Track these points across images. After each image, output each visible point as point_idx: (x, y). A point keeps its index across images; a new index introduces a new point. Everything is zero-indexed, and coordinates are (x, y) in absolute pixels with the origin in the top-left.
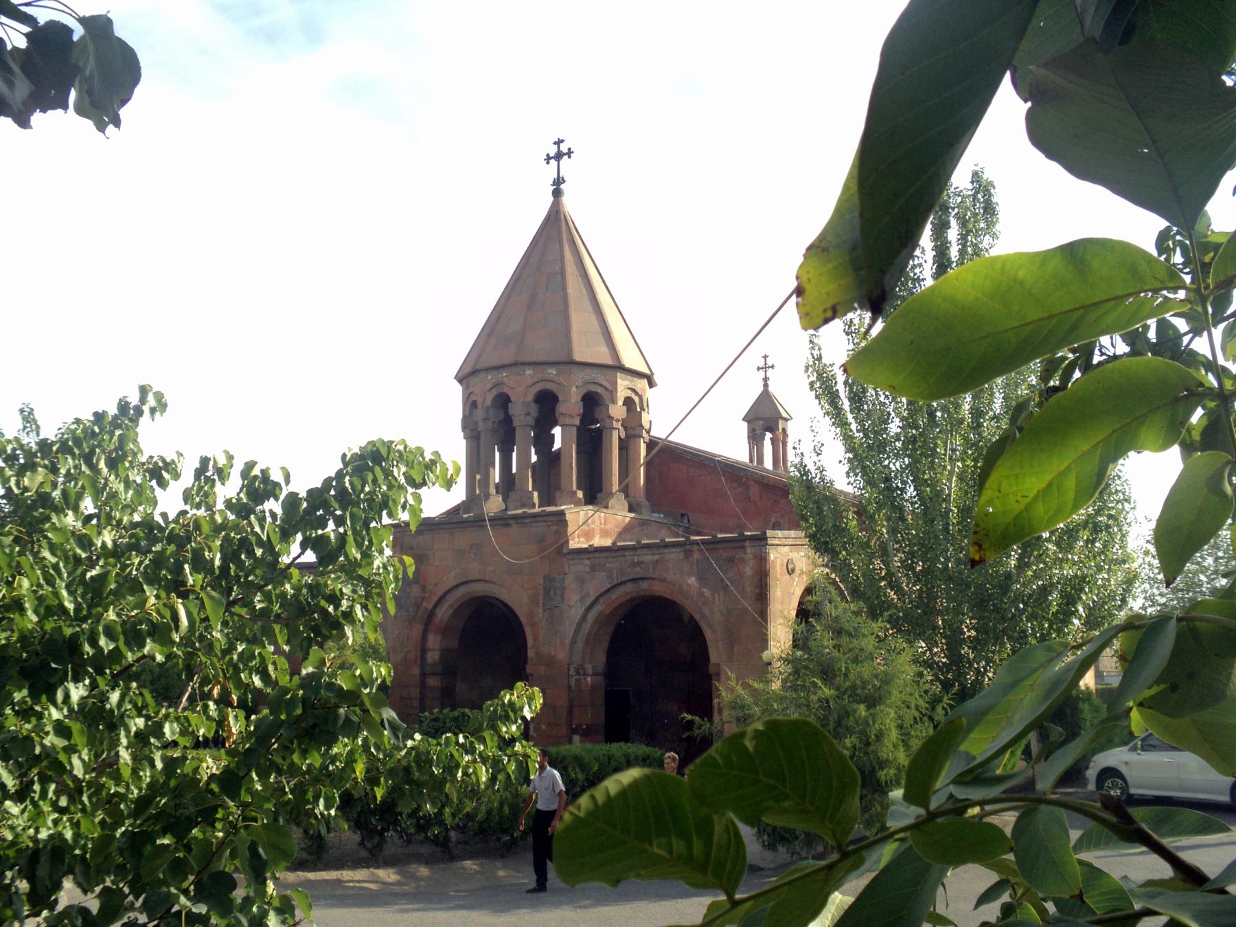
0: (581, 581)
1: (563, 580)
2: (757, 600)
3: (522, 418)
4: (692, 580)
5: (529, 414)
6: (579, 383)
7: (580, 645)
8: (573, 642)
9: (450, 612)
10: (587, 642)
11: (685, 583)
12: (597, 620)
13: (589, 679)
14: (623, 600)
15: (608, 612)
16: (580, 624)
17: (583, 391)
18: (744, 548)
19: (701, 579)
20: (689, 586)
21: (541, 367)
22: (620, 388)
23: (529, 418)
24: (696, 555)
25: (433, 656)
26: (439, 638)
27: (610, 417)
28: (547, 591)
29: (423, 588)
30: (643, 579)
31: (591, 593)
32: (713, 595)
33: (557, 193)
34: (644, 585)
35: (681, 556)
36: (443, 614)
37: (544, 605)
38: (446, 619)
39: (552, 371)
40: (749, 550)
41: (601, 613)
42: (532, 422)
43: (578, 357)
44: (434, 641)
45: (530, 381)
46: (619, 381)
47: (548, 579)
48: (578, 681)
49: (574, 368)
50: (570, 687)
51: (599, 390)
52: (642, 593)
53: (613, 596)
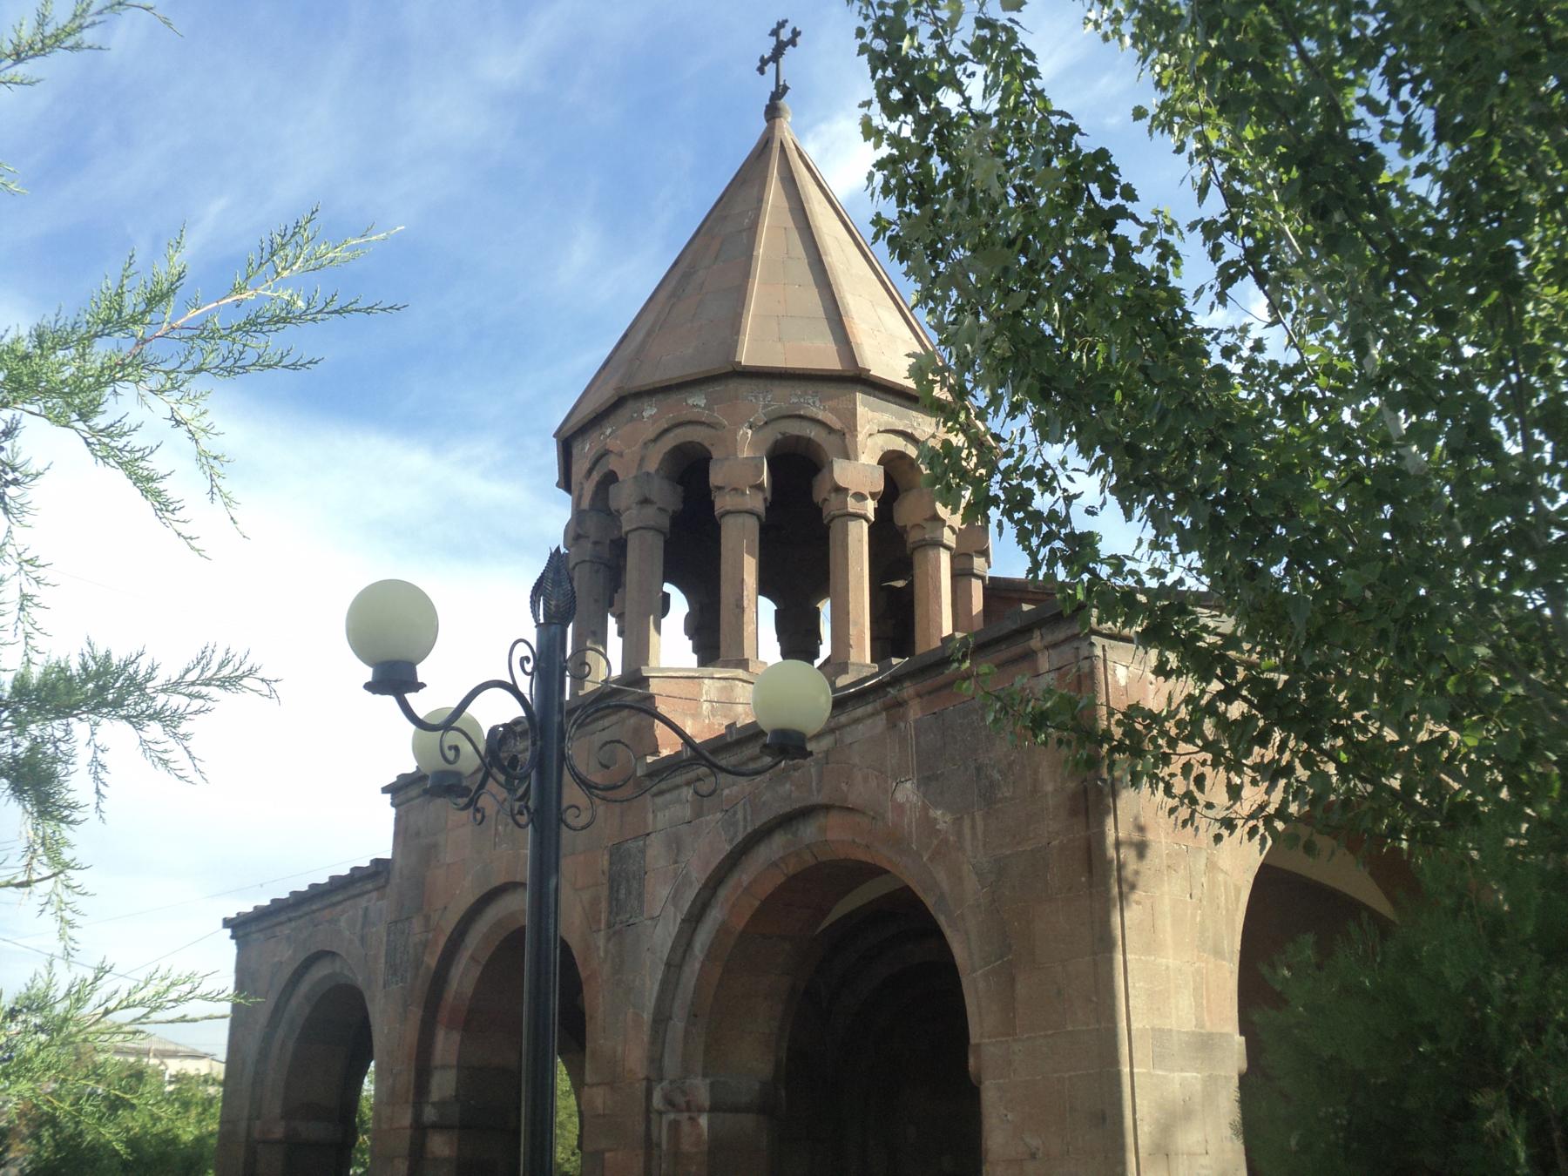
0: (676, 846)
1: (643, 851)
2: (1073, 812)
3: (634, 512)
4: (907, 792)
5: (645, 501)
6: (760, 416)
7: (678, 1025)
8: (661, 1019)
9: (476, 972)
10: (693, 1016)
11: (901, 810)
12: (710, 955)
13: (703, 1121)
14: (768, 888)
15: (740, 925)
16: (674, 966)
17: (772, 434)
18: (1029, 656)
19: (928, 780)
20: (900, 808)
21: (674, 398)
22: (863, 429)
23: (650, 511)
24: (914, 712)
25: (443, 1085)
26: (456, 1037)
27: (841, 491)
28: (614, 882)
29: (427, 918)
30: (806, 813)
31: (694, 875)
32: (958, 821)
33: (773, 112)
34: (809, 831)
35: (881, 722)
36: (463, 978)
37: (609, 926)
38: (469, 989)
39: (697, 400)
40: (1044, 663)
41: (723, 930)
42: (665, 522)
43: (747, 355)
44: (446, 1045)
45: (651, 432)
46: (860, 409)
47: (617, 853)
48: (675, 1126)
49: (744, 388)
50: (649, 1144)
51: (812, 432)
52: (809, 860)
53: (745, 875)
